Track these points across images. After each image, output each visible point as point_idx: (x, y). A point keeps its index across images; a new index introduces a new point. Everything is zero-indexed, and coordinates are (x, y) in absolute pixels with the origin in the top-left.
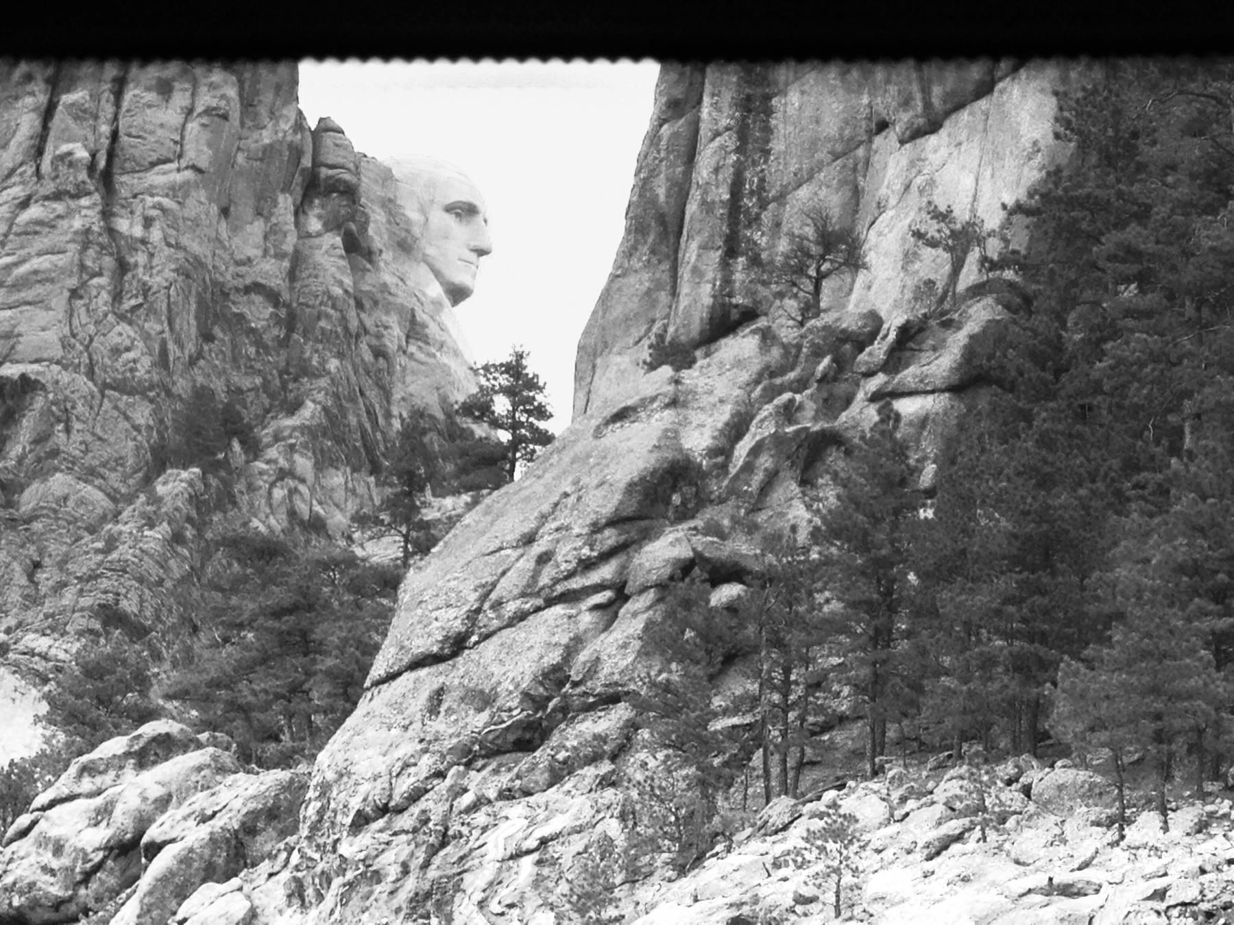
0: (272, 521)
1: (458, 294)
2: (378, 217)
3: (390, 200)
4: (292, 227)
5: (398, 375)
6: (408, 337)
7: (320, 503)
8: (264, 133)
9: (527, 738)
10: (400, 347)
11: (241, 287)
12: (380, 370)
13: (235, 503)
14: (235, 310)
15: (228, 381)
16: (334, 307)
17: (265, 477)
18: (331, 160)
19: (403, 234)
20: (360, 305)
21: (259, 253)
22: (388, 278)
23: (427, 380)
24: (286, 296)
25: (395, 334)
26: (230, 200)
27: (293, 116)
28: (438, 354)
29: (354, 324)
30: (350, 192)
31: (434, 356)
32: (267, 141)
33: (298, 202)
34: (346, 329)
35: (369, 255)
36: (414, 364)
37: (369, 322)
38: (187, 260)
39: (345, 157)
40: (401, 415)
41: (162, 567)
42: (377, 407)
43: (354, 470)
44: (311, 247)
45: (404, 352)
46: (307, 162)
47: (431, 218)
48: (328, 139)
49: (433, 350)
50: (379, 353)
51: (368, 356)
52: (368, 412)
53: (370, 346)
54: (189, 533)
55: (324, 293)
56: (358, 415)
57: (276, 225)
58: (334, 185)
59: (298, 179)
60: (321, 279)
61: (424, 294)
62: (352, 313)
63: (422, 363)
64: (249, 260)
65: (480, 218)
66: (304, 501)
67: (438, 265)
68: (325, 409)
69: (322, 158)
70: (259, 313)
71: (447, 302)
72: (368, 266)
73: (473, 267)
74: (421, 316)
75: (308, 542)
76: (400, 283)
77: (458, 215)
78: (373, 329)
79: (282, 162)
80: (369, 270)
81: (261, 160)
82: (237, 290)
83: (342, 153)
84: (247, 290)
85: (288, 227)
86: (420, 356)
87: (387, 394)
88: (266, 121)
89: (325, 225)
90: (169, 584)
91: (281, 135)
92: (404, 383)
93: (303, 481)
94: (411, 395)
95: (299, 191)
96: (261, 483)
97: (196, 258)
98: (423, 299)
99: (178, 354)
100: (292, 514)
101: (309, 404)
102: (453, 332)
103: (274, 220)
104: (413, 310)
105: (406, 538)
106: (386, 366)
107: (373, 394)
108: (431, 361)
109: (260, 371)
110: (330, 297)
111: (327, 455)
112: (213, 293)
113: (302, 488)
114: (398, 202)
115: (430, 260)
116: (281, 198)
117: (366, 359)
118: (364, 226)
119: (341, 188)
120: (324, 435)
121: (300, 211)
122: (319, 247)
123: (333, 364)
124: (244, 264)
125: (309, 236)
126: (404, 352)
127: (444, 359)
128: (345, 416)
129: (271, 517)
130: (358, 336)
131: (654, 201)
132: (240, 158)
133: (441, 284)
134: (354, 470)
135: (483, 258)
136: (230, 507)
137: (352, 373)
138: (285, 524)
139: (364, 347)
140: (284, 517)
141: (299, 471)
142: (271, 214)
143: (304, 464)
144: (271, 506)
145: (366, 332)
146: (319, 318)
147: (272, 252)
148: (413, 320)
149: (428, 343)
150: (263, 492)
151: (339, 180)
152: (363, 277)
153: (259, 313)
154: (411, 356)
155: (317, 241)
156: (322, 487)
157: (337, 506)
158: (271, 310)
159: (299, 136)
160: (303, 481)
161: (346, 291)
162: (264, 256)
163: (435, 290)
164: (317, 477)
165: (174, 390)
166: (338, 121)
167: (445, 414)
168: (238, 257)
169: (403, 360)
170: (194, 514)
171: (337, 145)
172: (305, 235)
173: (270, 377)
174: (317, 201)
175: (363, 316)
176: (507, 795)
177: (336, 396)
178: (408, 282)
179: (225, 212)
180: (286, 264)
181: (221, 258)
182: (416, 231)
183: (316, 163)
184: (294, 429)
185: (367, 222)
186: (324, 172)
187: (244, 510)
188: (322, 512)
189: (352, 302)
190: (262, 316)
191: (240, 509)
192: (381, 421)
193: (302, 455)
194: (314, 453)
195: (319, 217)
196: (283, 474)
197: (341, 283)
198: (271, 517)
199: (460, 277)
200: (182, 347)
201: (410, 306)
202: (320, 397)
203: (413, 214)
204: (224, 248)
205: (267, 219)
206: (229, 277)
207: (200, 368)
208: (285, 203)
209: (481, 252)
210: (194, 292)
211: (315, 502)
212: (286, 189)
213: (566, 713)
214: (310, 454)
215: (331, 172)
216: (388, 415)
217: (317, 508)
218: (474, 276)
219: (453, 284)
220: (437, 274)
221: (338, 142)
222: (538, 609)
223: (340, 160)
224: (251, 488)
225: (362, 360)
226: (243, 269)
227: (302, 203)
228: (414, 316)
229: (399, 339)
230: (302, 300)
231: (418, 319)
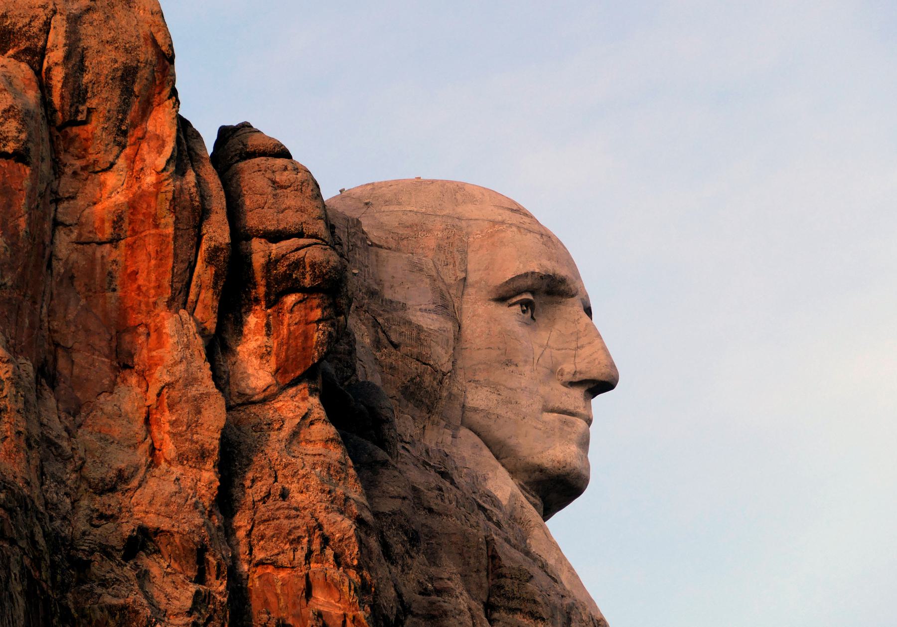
4: (209, 385)
8: (111, 179)
14: (108, 600)
21: (141, 456)
22: (416, 476)
27: (169, 132)
32: (120, 198)
33: (211, 325)
37: (410, 590)
39: (302, 210)
44: (257, 428)
46: (217, 231)
47: (466, 322)
55: (310, 532)
57: (169, 385)
58: (287, 277)
59: (203, 272)
60: (297, 498)
64: (122, 477)
65: (574, 308)
67: (500, 432)
72: (381, 454)
73: (581, 423)
77: (527, 305)
78: (418, 602)
79: (162, 240)
80: (385, 464)
82: (106, 551)
85: (193, 391)
89: (280, 371)
91: (150, 179)
95: (206, 300)
102: (564, 577)
103: (161, 376)
104: (489, 542)
112: (53, 566)
114: (388, 295)
115: (476, 418)
116: (170, 325)
119: (307, 282)
121: (218, 346)
124: (113, 489)
125: (248, 402)
132: (63, 244)
133: (513, 473)
135: (600, 401)
142: (153, 364)
146: (308, 592)
147: (169, 449)
151: (297, 264)
159: (191, 177)
161: (360, 521)
166: (271, 126)
168: (95, 473)
172: (238, 402)
174: (253, 321)
178: (457, 480)
179: (46, 375)
180: (209, 475)
182: (441, 356)
183: (240, 234)
189: (373, 543)
195: (264, 355)
199: (555, 453)
204: (66, 459)
206: (82, 525)
209: (600, 385)
210: (16, 570)
212: (180, 298)
215: (276, 249)
218: (584, 443)
219: (541, 469)
220: (500, 451)
221: (281, 178)
223: (290, 220)
226: (112, 501)
228: (494, 557)
230: (260, 555)
231: (506, 562)
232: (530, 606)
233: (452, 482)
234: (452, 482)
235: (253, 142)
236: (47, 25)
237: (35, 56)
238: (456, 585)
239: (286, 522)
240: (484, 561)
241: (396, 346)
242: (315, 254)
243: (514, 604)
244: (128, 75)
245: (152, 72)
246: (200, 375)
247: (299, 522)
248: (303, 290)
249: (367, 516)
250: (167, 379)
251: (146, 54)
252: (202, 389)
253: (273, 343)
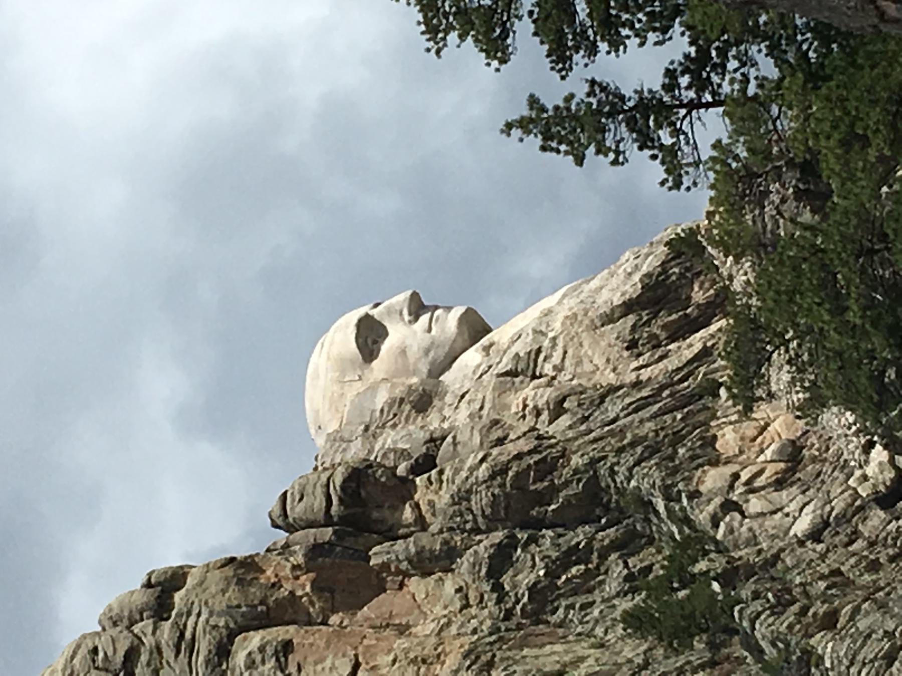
0: (793, 507)
2: (389, 439)
3: (367, 429)
5: (584, 382)
6: (534, 377)
7: (762, 451)
8: (299, 593)
10: (549, 384)
11: (495, 595)
12: (579, 405)
13: (777, 557)
15: (618, 595)
16: (504, 471)
17: (736, 524)
18: (319, 502)
19: (407, 407)
20: (500, 441)
23: (586, 344)
24: (498, 536)
25: (533, 393)
26: (388, 625)
28: (551, 335)
29: (524, 445)
30: (359, 477)
31: (554, 339)
34: (530, 453)
35: (435, 441)
36: (567, 363)
38: (469, 667)
39: (315, 485)
40: (638, 369)
41: (869, 636)
42: (628, 400)
43: (714, 417)
45: (554, 378)
48: (296, 510)
49: (546, 343)
50: (558, 409)
51: (564, 421)
52: (636, 411)
53: (550, 423)
54: (820, 608)
56: (641, 421)
57: (410, 562)
59: (349, 542)
61: (479, 366)
62: (512, 449)
63: (565, 352)
66: (761, 472)
68: (638, 463)
69: (321, 516)
71: (485, 341)
72: (449, 439)
74: (506, 364)
75: (814, 460)
76: (467, 397)
78: (530, 421)
80: (454, 438)
81: (332, 592)
82: (499, 601)
83: (309, 489)
84: (498, 587)
86: (556, 358)
87: (613, 389)
88: (284, 593)
90: (890, 625)
92: (593, 372)
93: (736, 476)
94: (608, 361)
96: (744, 529)
97: (466, 656)
98: (484, 367)
99: (591, 661)
100: (780, 484)
101: (633, 483)
103: (404, 565)
105: (693, 106)
106: (572, 398)
107: (613, 408)
108: (560, 343)
109: (600, 557)
110: (492, 477)
111: (698, 451)
112: (507, 630)
113: (745, 476)
117: (569, 423)
118: (403, 454)
119: (354, 485)
120: (671, 458)
121: (391, 535)
122: (431, 504)
123: (576, 460)
126: (554, 378)
127: (557, 325)
128: (645, 438)
129: (786, 510)
130: (539, 437)
133: (464, 350)
134: (714, 417)
136: (780, 566)
137: (586, 438)
138: (794, 490)
139: (551, 429)
140: (784, 493)
141: (723, 483)
142: (399, 572)
143: (712, 479)
144: (774, 512)
145: (533, 429)
148: (512, 374)
149: (539, 351)
150: (755, 525)
152: (465, 445)
154: (559, 369)
155: (424, 508)
156: (741, 452)
157: (764, 429)
158: (519, 550)
160: (736, 476)
162: (452, 570)
163: (472, 357)
164: (728, 462)
165: (639, 660)
167: (625, 315)
168: (458, 605)
169: (564, 377)
170: (795, 608)
171: (301, 499)
173: (606, 542)
174: (375, 515)
175: (512, 436)
177: (620, 451)
179: (403, 630)
181: (462, 625)
183: (328, 521)
184: (668, 498)
185: (395, 451)
187: (781, 544)
188: (773, 447)
189: (495, 451)
190: (529, 564)
191: (782, 550)
192: (645, 393)
193: (700, 481)
194: (696, 468)
196: (729, 506)
197: (472, 470)
198: (786, 510)
200: (582, 659)
201: (494, 380)
202: (622, 470)
203: (382, 398)
205: (407, 575)
207: (606, 632)
211: (762, 458)
214: (699, 473)
216: (637, 385)
217: (768, 454)
224: (753, 540)
225: (570, 427)
227: (378, 533)
229: (538, 387)
231: (508, 368)
232: (533, 356)
233: (467, 392)
234: (467, 392)
235: (277, 511)
236: (215, 627)
237: (232, 636)
238: (522, 395)
239: (484, 502)
240: (509, 378)
241: (395, 415)
242: (338, 479)
243: (532, 365)
244: (240, 582)
246: (404, 546)
247: (484, 493)
248: (358, 486)
249: (480, 455)
250: (405, 563)
251: (229, 571)
252: (411, 545)
253: (387, 505)
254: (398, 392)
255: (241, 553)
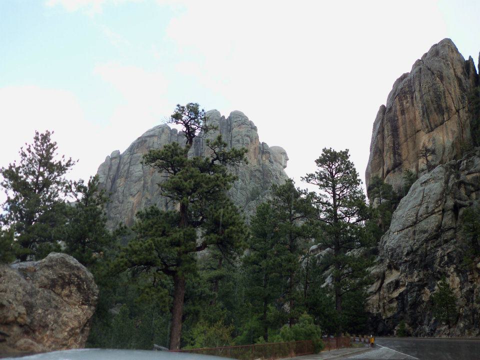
1: (285, 167)
9: (436, 237)
24: (262, 171)
25: (278, 175)
48: (264, 145)
50: (277, 178)
70: (258, 174)
131: (378, 148)
153: (258, 174)
176: (436, 247)
180: (261, 166)
186: (265, 150)
208: (260, 156)
213: (443, 231)
222: (429, 216)
245: (257, 138)
254: (277, 158)
255: (260, 138)
